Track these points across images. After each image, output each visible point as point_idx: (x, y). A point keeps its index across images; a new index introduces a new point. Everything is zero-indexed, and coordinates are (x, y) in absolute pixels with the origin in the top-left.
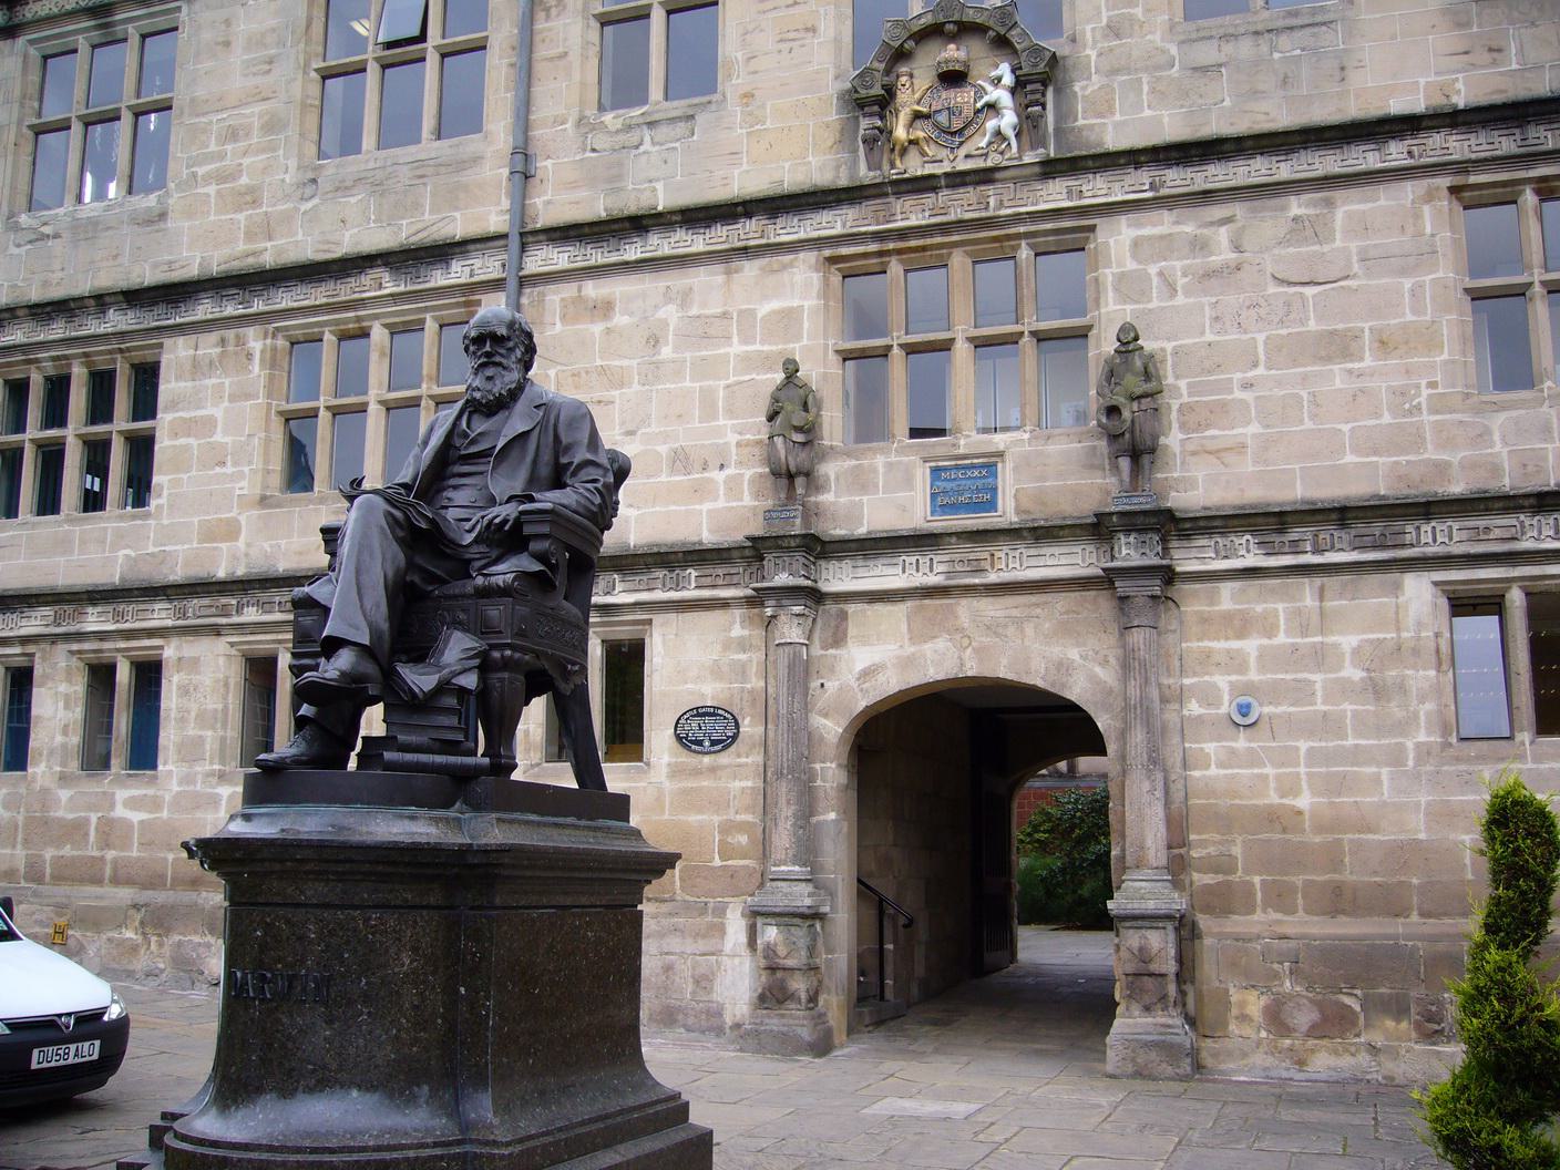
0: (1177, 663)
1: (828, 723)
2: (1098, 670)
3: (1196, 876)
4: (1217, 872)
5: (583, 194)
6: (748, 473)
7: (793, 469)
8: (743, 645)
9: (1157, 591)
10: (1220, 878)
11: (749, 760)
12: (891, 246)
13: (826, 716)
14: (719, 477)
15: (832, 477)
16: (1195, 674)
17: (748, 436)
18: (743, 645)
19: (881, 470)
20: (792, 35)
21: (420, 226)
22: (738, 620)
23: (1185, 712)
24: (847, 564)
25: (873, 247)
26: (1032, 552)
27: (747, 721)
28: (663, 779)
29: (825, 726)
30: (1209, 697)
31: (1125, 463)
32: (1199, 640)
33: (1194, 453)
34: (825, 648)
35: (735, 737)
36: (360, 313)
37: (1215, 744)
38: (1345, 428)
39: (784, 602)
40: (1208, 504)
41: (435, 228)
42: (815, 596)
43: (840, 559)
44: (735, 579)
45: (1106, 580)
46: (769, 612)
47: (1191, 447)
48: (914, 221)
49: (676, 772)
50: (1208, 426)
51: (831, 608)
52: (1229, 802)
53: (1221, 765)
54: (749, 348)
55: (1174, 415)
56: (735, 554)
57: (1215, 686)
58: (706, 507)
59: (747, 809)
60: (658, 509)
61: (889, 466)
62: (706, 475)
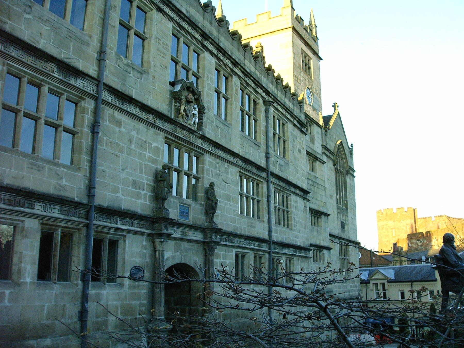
5: (116, 80)
12: (176, 140)
14: (143, 192)
18: (145, 248)
20: (162, 66)
21: (68, 57)
25: (173, 139)
26: (193, 232)
28: (127, 290)
36: (45, 79)
38: (229, 216)
41: (73, 61)
48: (180, 136)
49: (130, 287)
54: (150, 155)
58: (139, 201)
60: (129, 198)
62: (140, 191)
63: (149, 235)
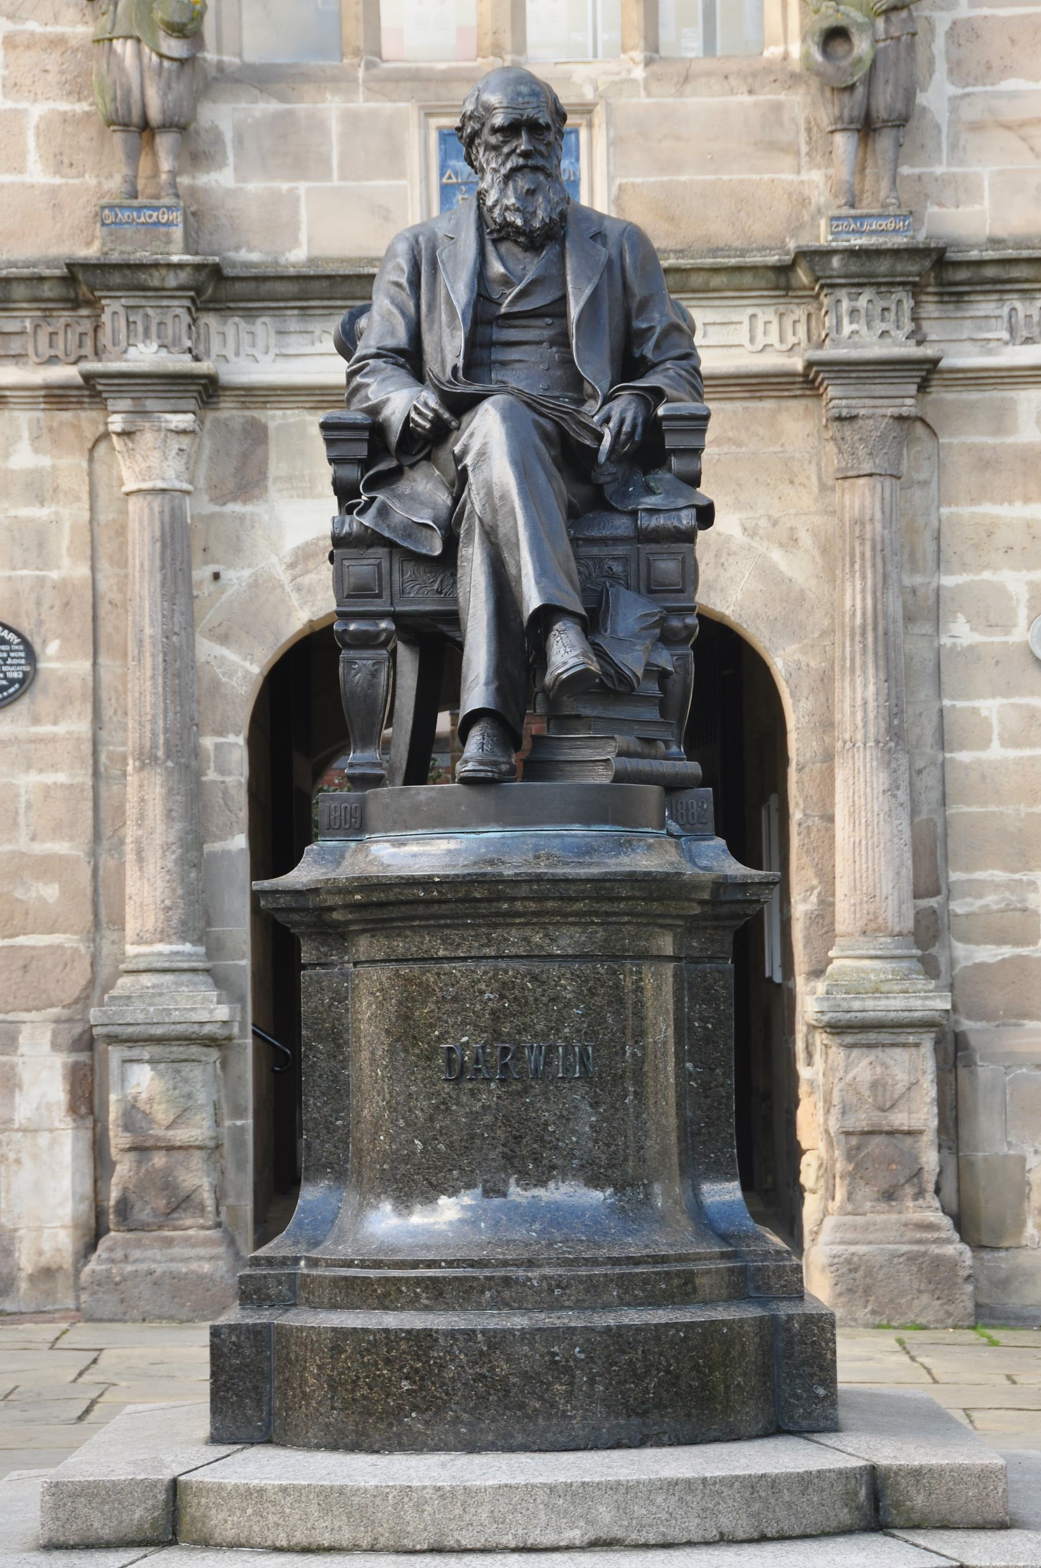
0: (930, 546)
1: (230, 655)
2: (777, 556)
3: (960, 949)
4: (1000, 942)
6: (37, 111)
7: (155, 115)
8: (38, 488)
9: (908, 407)
10: (1007, 951)
11: (61, 729)
13: (224, 639)
15: (228, 136)
16: (964, 567)
17: (32, 26)
18: (38, 488)
19: (335, 127)
22: (26, 434)
23: (945, 640)
24: (264, 327)
27: (53, 647)
29: (222, 660)
30: (993, 619)
31: (844, 143)
32: (973, 501)
33: (976, 127)
34: (221, 498)
35: (25, 683)
37: (999, 701)
39: (150, 404)
40: (1000, 233)
42: (207, 390)
43: (250, 314)
44: (15, 346)
45: (809, 381)
46: (117, 422)
47: (969, 113)
50: (1007, 71)
51: (228, 411)
52: (1023, 809)
53: (1010, 741)
55: (939, 45)
56: (19, 291)
57: (1001, 590)
59: (57, 831)
61: (352, 121)
63: (56, 396)
